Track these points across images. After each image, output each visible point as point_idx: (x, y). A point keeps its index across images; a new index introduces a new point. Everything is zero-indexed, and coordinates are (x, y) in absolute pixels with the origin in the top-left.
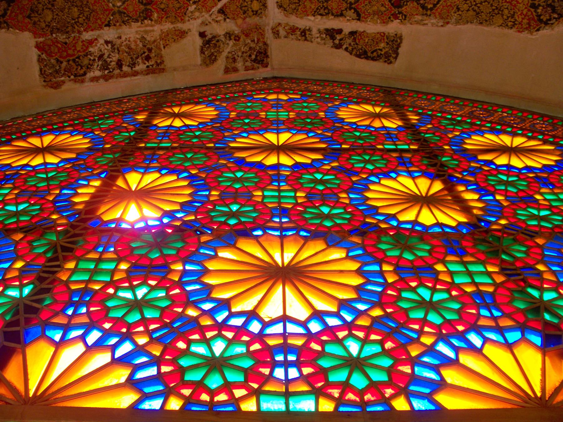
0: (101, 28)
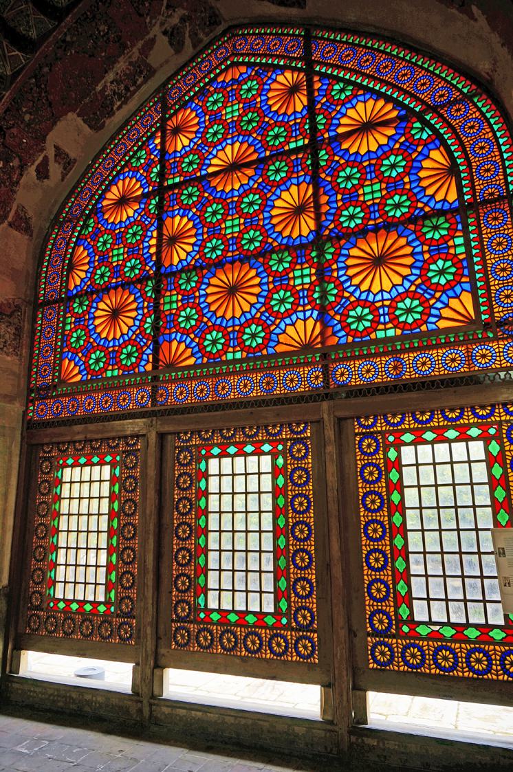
0: (103, 77)
